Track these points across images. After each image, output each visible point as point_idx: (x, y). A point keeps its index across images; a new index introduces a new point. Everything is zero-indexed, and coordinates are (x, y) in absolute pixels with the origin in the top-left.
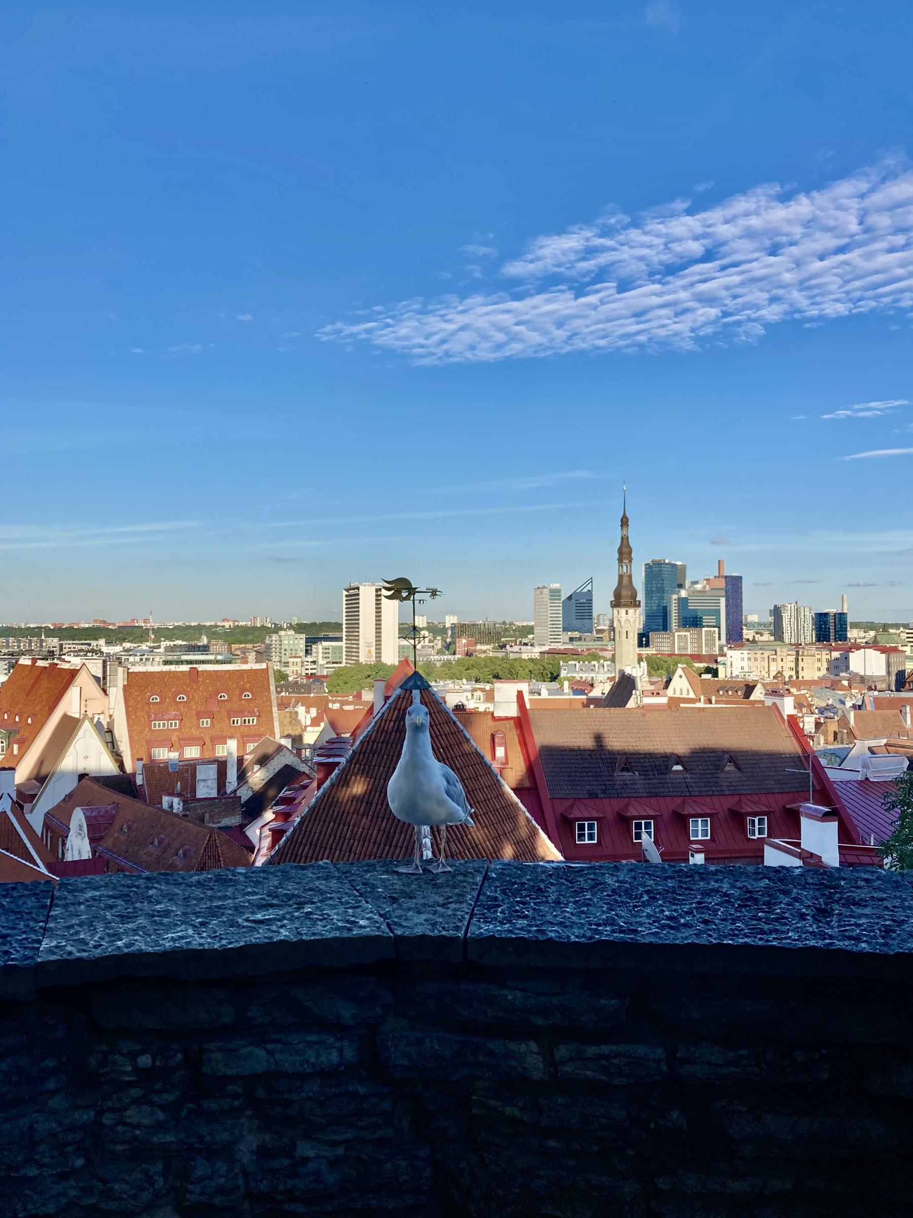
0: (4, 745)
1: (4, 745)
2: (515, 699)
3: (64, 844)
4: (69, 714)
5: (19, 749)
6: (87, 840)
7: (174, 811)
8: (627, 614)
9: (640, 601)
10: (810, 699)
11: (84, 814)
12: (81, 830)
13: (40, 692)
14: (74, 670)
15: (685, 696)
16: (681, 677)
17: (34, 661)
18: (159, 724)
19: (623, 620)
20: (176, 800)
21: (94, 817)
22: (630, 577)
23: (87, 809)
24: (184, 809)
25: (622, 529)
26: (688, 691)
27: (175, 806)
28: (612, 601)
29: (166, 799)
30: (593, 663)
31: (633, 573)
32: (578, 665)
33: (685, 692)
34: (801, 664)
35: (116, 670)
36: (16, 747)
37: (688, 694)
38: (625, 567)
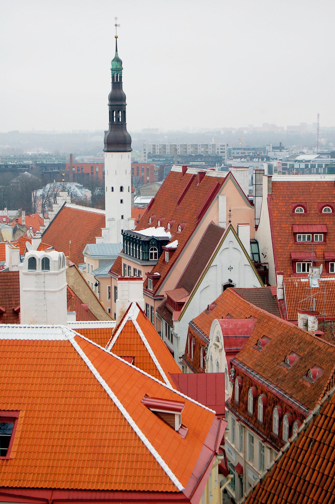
0: (157, 252)
1: (157, 252)
3: (204, 354)
4: (216, 223)
5: (170, 257)
6: (224, 353)
7: (309, 329)
11: (221, 326)
12: (218, 341)
13: (190, 200)
14: (220, 178)
17: (185, 169)
18: (304, 237)
20: (311, 319)
21: (231, 329)
23: (224, 321)
24: (319, 329)
27: (310, 324)
29: (301, 317)
35: (261, 180)
36: (167, 254)
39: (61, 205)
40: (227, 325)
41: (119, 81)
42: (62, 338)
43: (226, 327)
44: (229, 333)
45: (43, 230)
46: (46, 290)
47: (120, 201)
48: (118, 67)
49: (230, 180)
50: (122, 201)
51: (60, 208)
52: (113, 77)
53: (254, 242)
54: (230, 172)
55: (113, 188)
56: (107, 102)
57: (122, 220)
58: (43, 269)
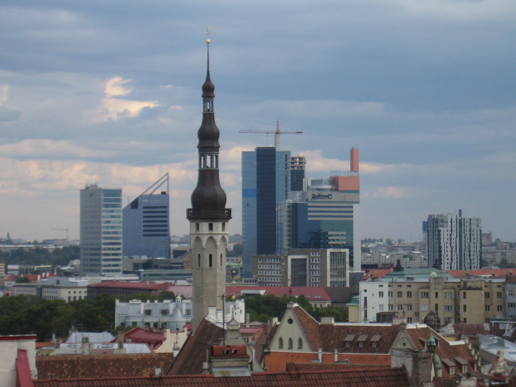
2: (12, 363)
8: (211, 227)
9: (230, 210)
10: (473, 352)
15: (295, 350)
16: (290, 321)
19: (204, 239)
22: (218, 171)
25: (205, 102)
26: (300, 341)
28: (188, 210)
30: (165, 301)
31: (220, 167)
32: (143, 304)
33: (296, 344)
34: (463, 302)
37: (300, 346)
38: (209, 158)
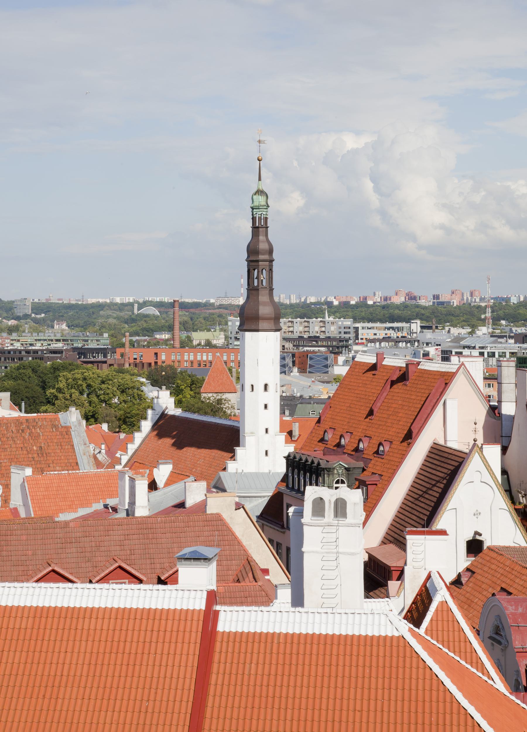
4: (442, 442)
12: (497, 633)
39: (159, 412)
40: (514, 607)
41: (262, 224)
42: (389, 631)
43: (513, 611)
44: (520, 620)
45: (132, 449)
46: (340, 550)
47: (264, 407)
48: (263, 203)
49: (462, 376)
50: (266, 406)
51: (158, 416)
52: (254, 219)
53: (504, 472)
54: (463, 364)
55: (252, 386)
56: (245, 256)
57: (267, 435)
58: (336, 515)
